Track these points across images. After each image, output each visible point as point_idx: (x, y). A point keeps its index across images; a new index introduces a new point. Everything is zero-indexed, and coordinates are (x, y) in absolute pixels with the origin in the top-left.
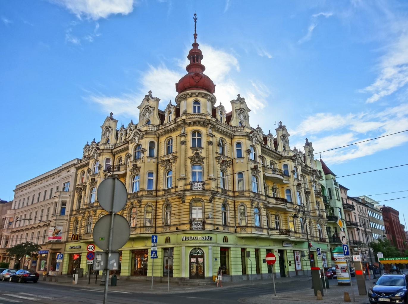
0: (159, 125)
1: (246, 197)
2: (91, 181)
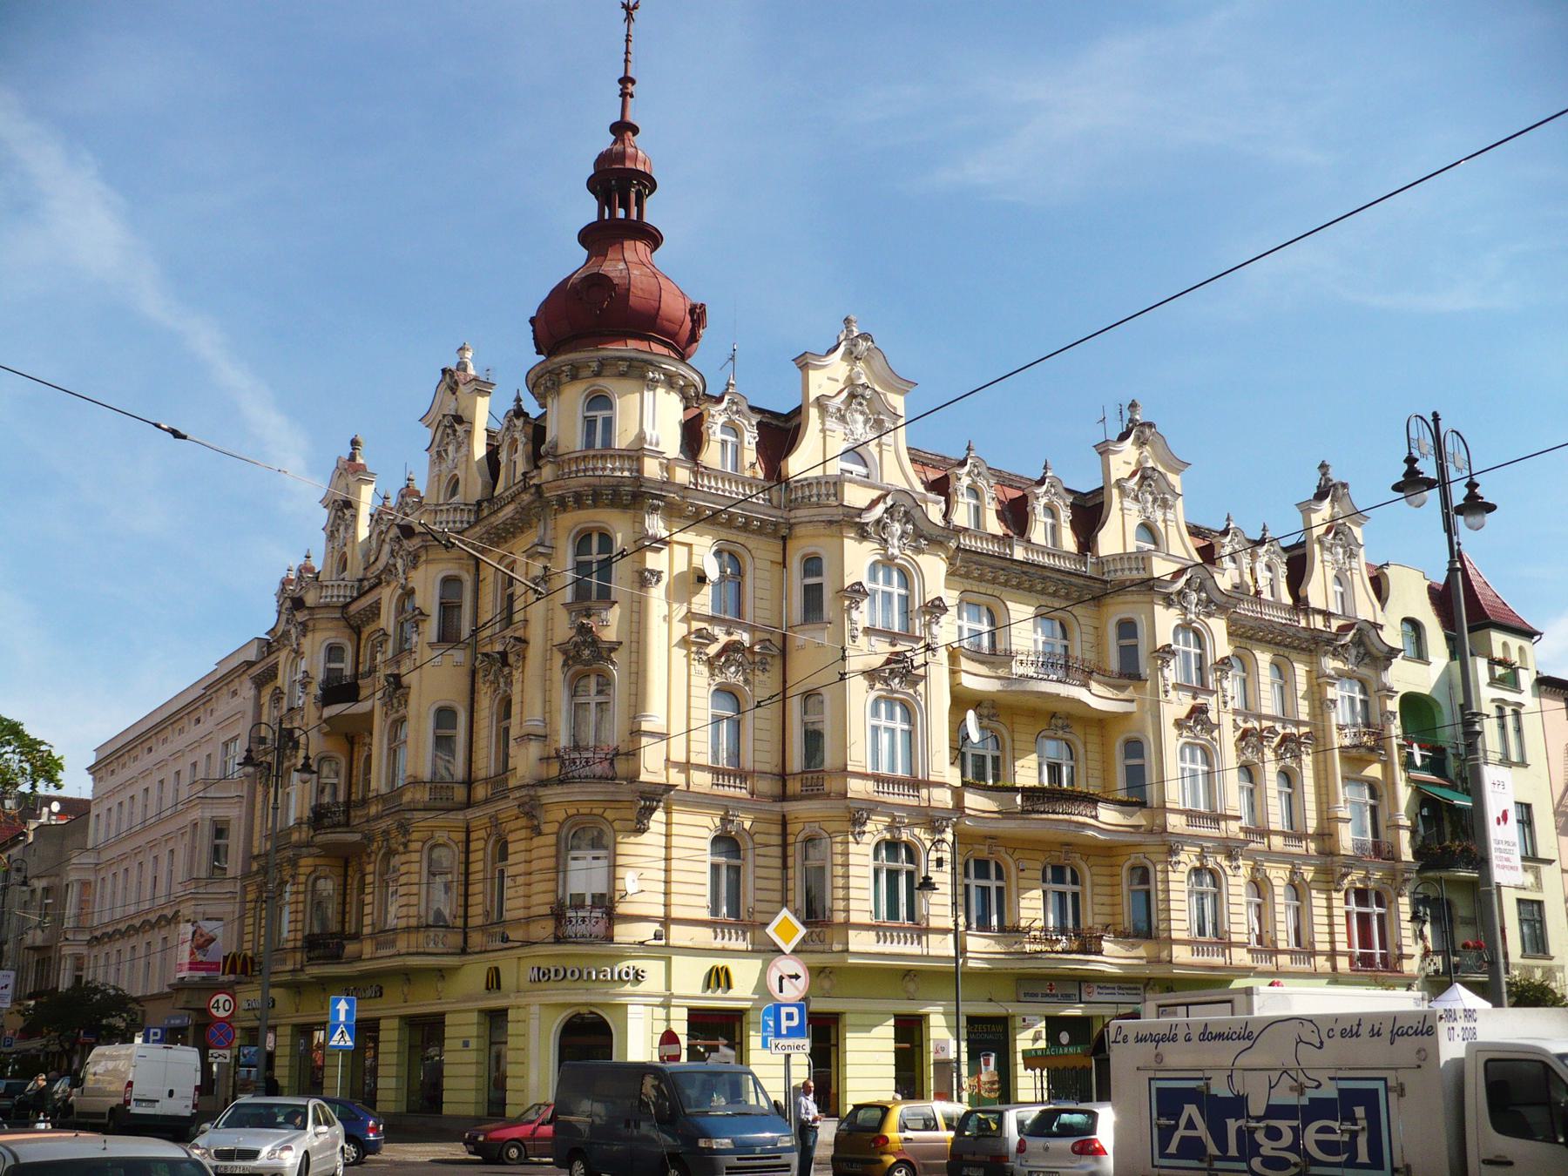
0: (479, 503)
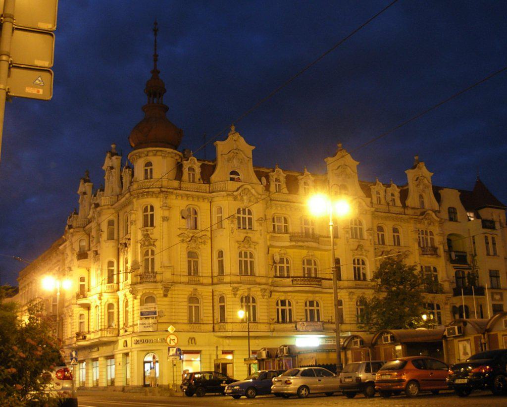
1: (225, 283)
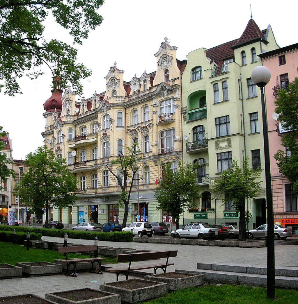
2: (56, 149)
